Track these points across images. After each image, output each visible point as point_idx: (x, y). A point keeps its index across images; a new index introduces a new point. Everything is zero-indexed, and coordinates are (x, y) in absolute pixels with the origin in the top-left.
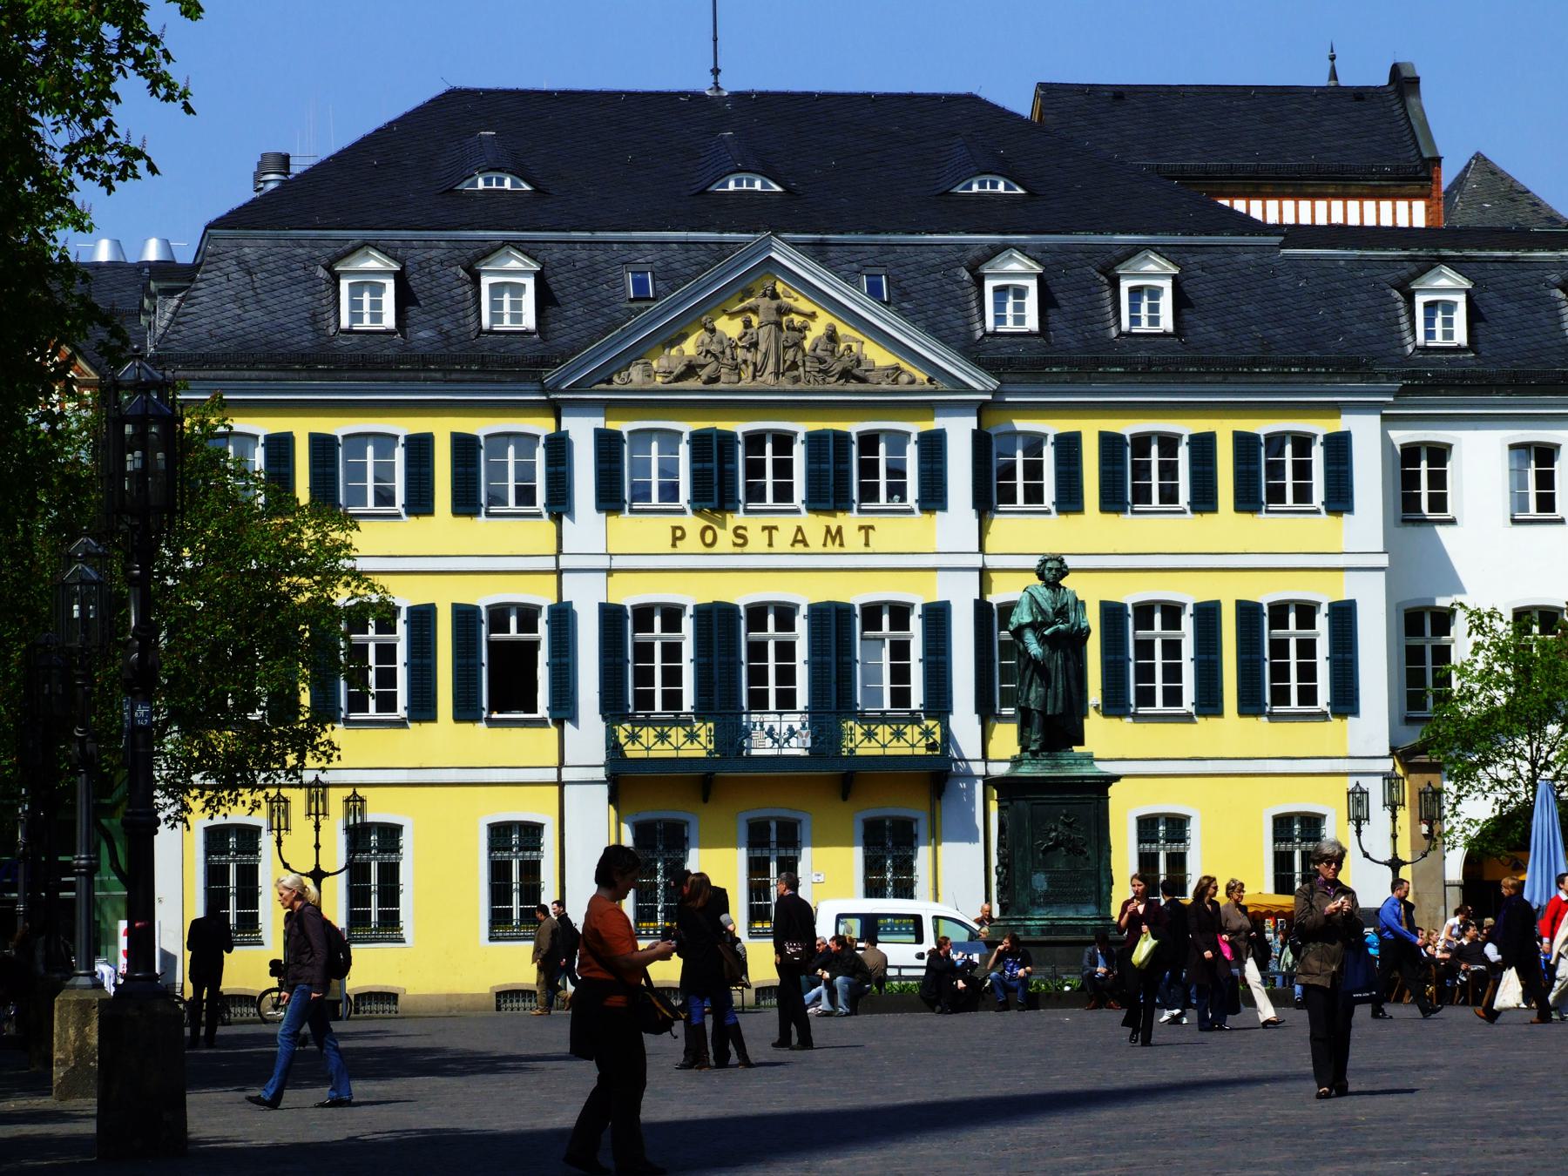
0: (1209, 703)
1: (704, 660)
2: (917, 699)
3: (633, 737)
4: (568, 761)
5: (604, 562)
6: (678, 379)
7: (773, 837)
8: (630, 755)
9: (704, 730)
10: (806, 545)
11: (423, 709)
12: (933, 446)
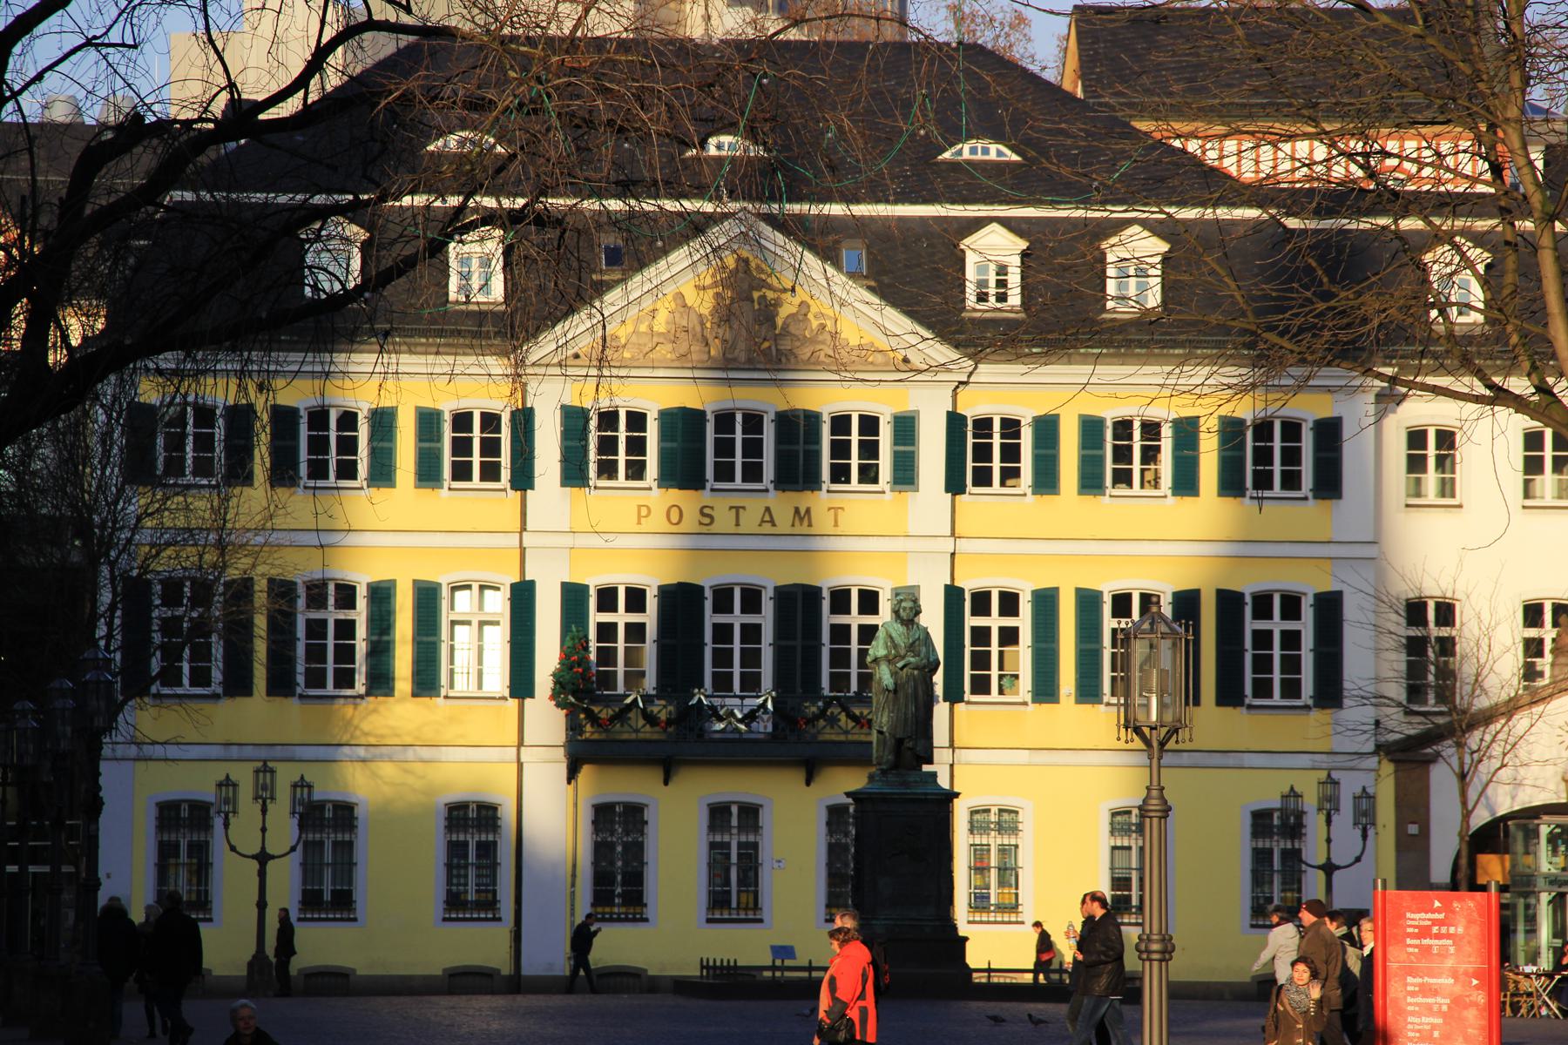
4: (527, 741)
7: (734, 822)
10: (774, 525)
12: (906, 427)
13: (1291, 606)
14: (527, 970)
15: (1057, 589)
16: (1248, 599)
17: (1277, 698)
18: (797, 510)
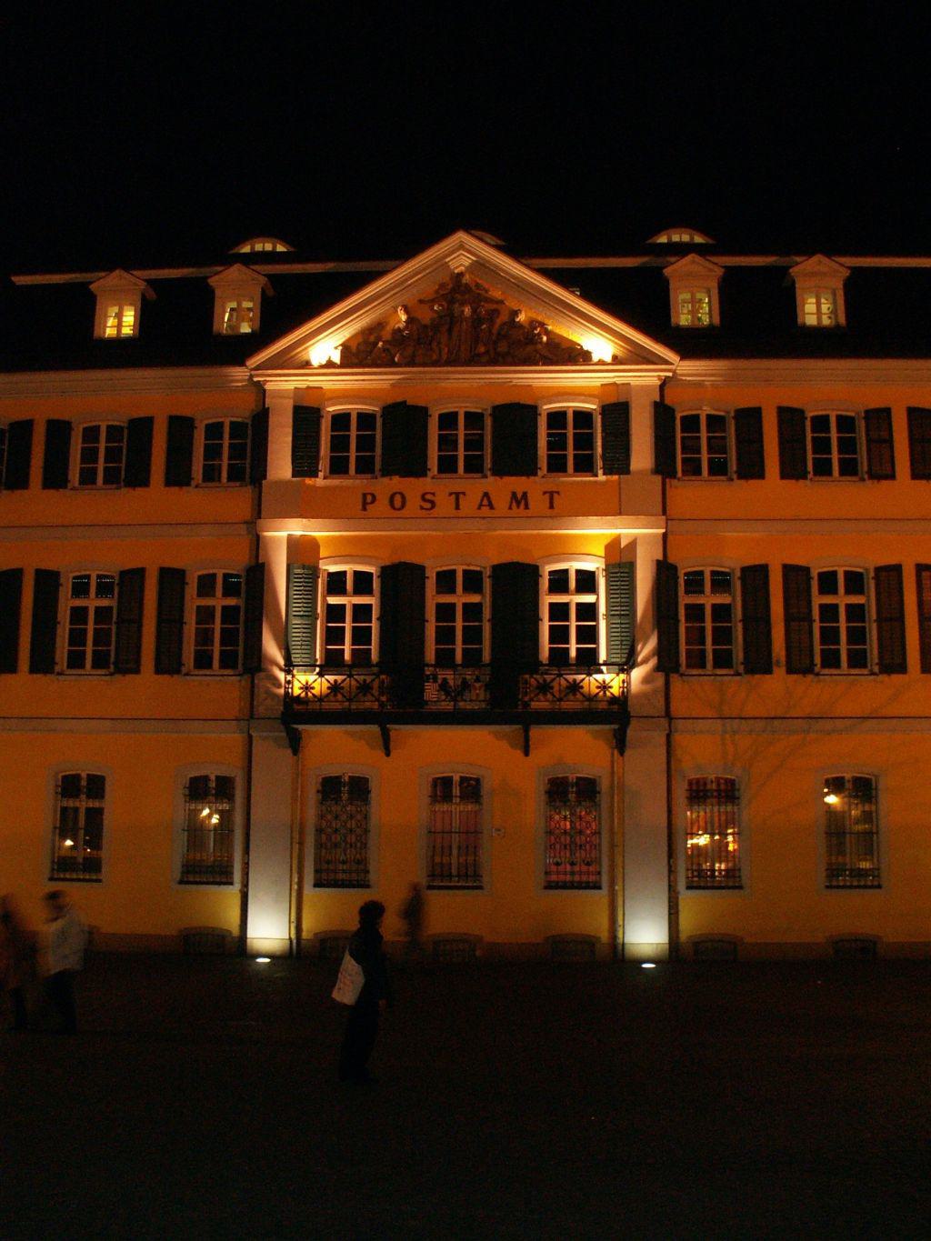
18: (514, 494)
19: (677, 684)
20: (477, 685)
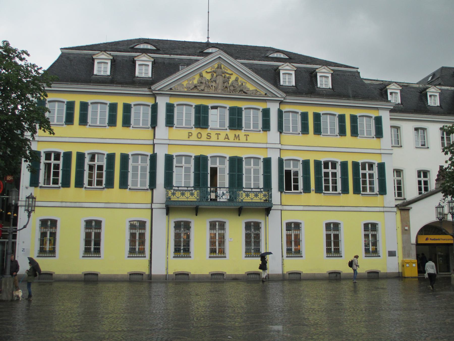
0: (345, 190)
1: (197, 172)
2: (261, 186)
3: (174, 194)
4: (154, 202)
5: (167, 142)
6: (191, 89)
7: (217, 227)
8: (172, 199)
9: (196, 193)
10: (229, 139)
11: (110, 184)
12: (266, 113)
13: (371, 166)
14: (153, 273)
15: (309, 160)
16: (360, 164)
17: (368, 192)
18: (235, 135)
19: (283, 194)
20: (227, 194)
